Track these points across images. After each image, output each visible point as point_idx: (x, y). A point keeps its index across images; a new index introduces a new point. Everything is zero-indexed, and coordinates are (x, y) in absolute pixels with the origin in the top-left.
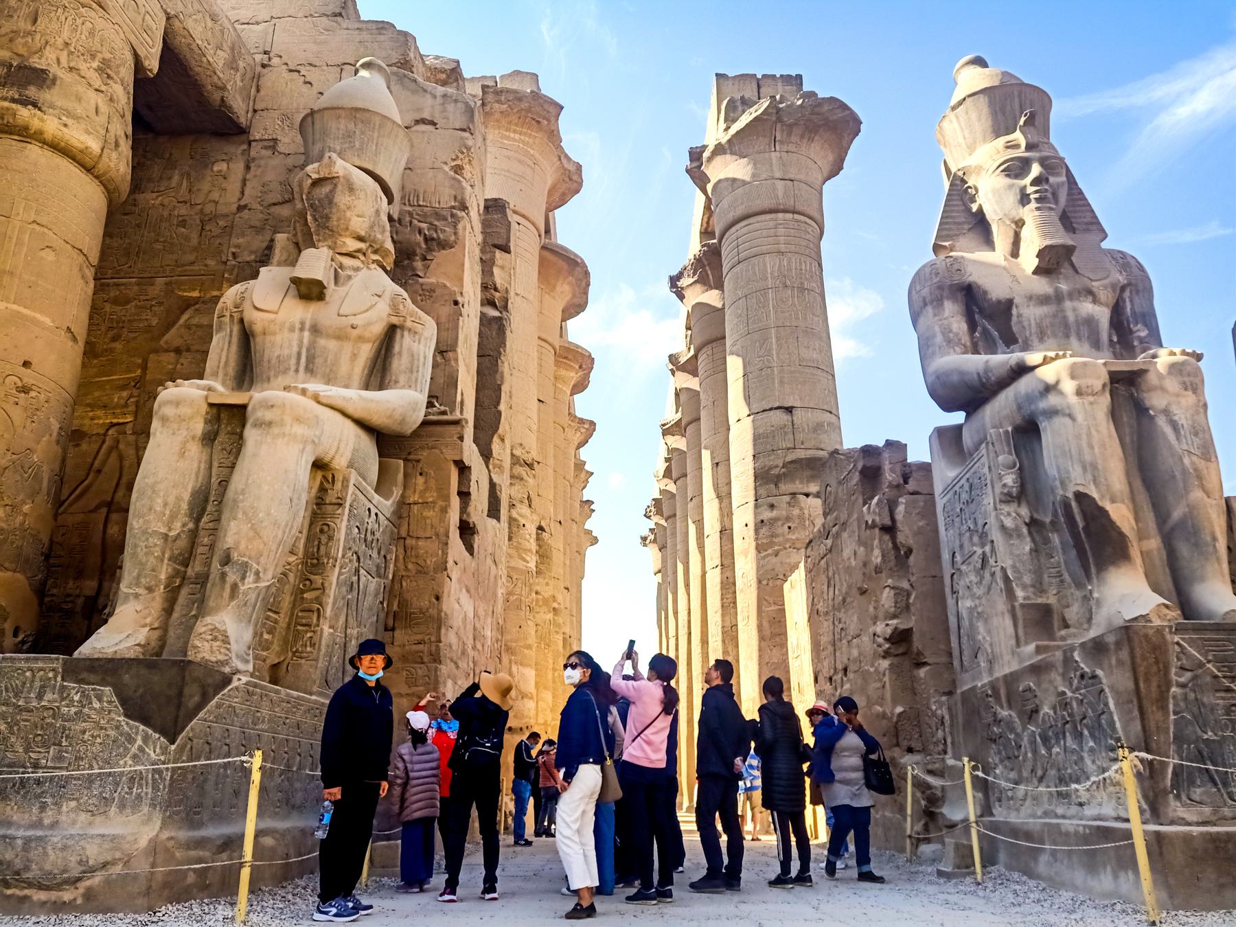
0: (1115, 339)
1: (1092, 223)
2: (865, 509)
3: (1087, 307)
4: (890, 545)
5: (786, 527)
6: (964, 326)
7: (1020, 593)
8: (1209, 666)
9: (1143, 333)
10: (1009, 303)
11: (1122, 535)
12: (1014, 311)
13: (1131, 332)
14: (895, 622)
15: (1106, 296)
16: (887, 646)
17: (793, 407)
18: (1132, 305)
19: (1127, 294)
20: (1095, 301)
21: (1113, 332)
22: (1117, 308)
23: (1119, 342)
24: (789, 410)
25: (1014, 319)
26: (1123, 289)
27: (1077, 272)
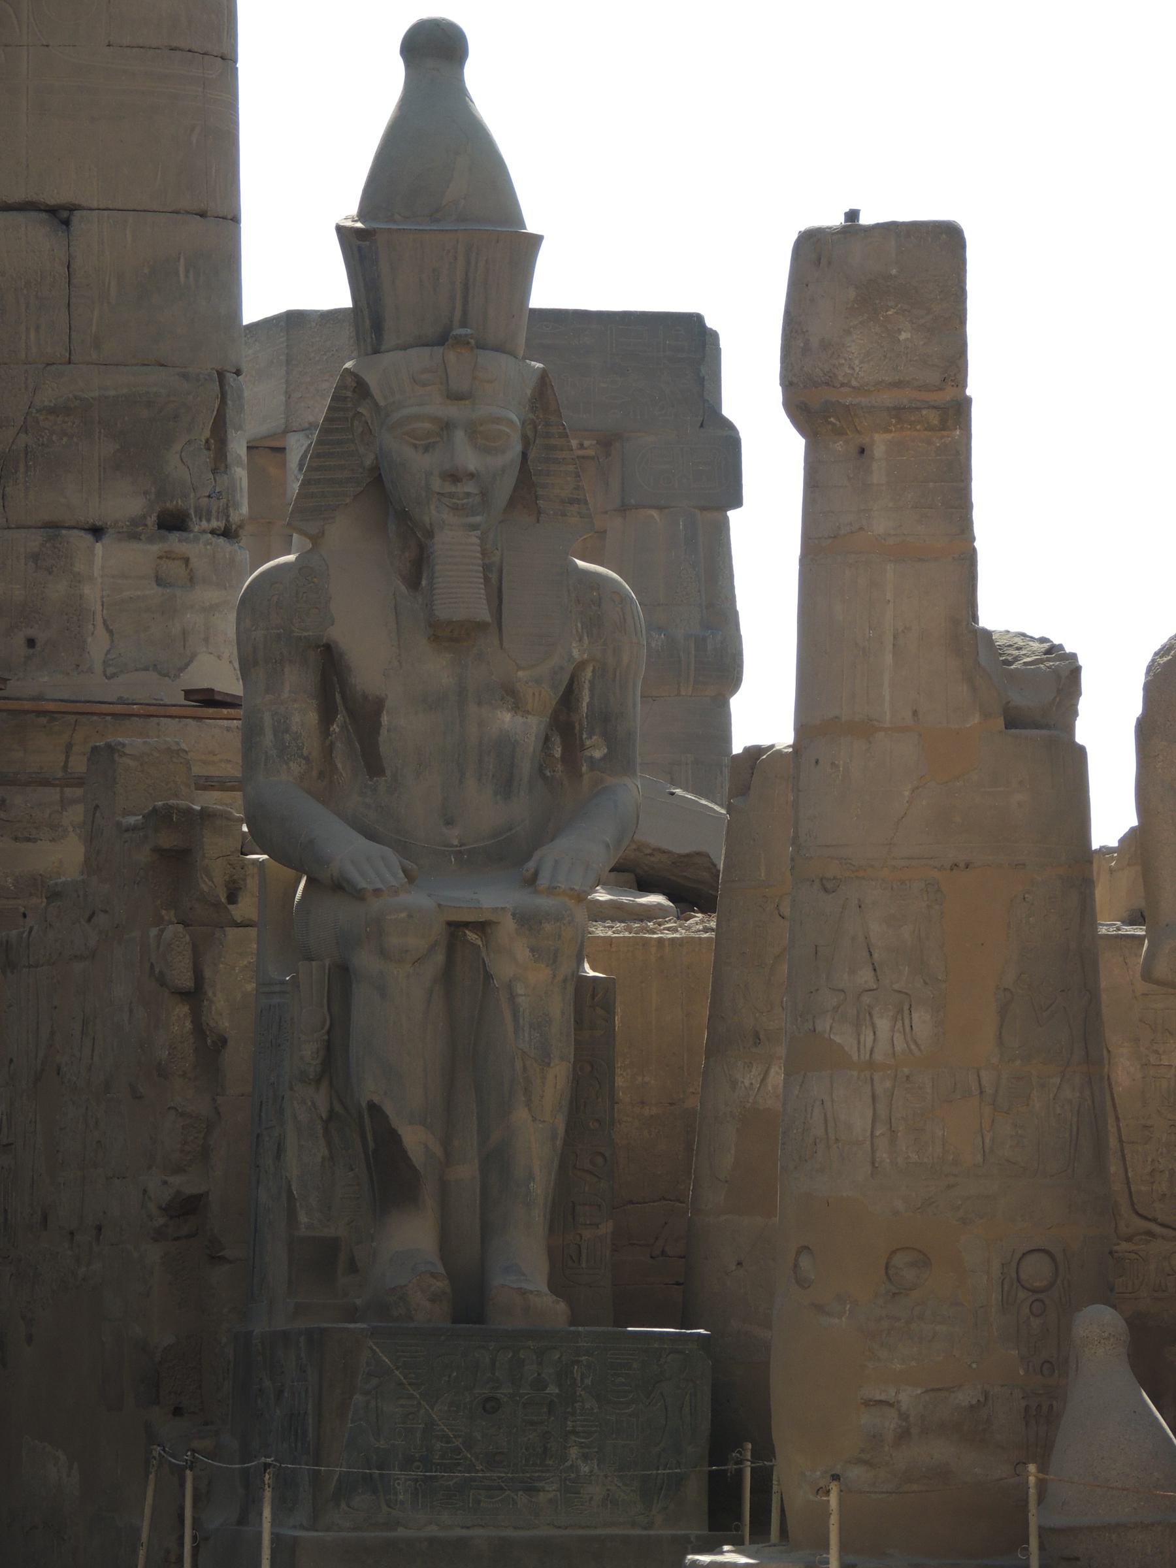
0: (558, 752)
1: (572, 502)
2: (154, 932)
3: (506, 719)
4: (188, 1025)
5: (19, 639)
6: (313, 717)
7: (303, 1218)
8: (397, 1373)
9: (597, 754)
10: (379, 704)
11: (412, 1167)
12: (385, 719)
13: (582, 747)
14: (176, 1180)
15: (543, 698)
16: (161, 1221)
17: (73, 208)
18: (592, 697)
19: (588, 673)
20: (518, 706)
21: (557, 740)
22: (568, 698)
23: (563, 759)
24: (61, 216)
25: (384, 732)
26: (581, 665)
27: (501, 644)
